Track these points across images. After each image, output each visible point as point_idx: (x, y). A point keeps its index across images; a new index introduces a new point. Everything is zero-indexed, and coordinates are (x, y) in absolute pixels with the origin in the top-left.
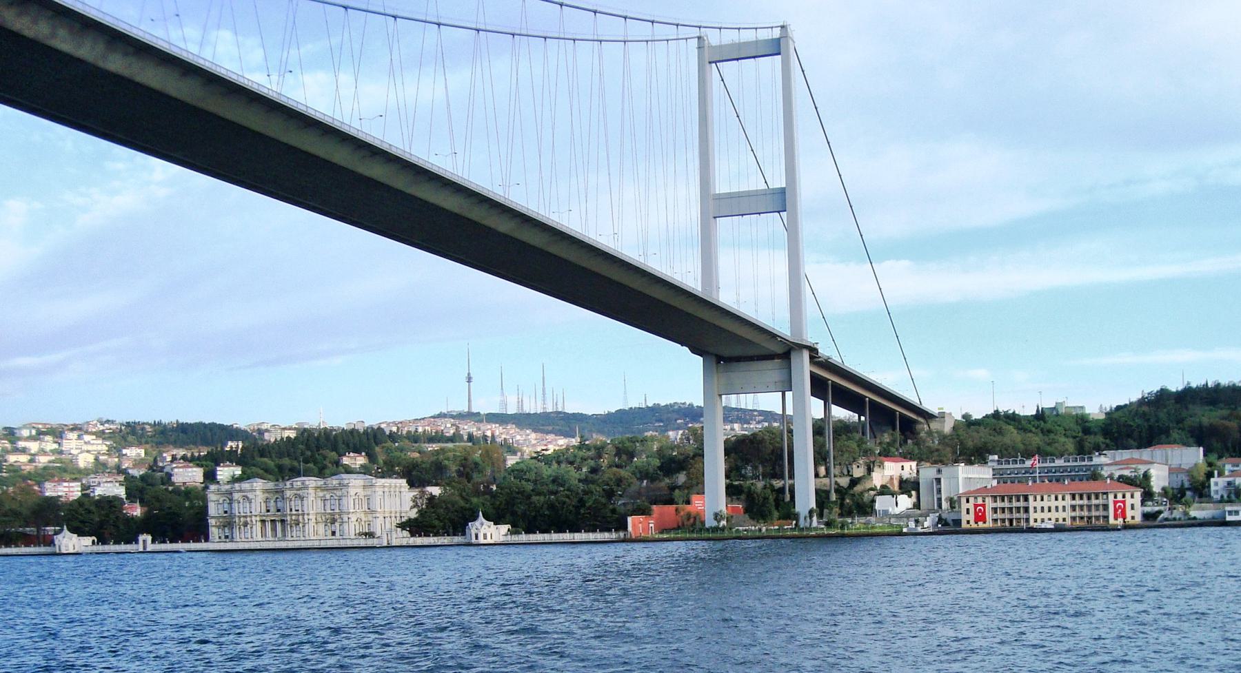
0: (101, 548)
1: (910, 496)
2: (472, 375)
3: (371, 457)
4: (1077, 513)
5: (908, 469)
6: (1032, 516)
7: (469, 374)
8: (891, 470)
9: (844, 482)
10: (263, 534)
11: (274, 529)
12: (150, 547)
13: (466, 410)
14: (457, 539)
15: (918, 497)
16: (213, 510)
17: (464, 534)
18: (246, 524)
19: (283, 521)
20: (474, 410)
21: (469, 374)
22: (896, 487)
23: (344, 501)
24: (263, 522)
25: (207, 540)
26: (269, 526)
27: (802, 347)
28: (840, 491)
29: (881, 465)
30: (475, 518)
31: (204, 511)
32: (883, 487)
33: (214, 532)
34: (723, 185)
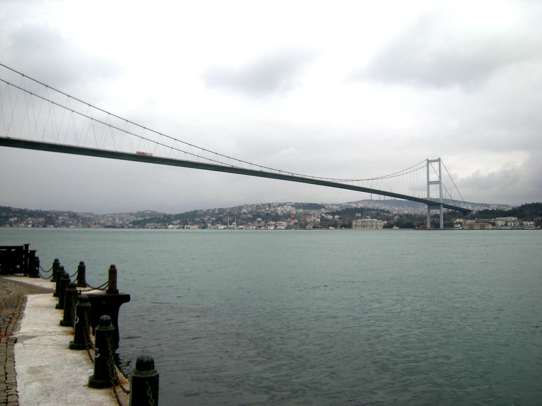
0: (335, 229)
1: (460, 225)
3: (362, 214)
4: (481, 228)
5: (461, 220)
6: (474, 228)
8: (458, 220)
9: (450, 222)
10: (362, 228)
11: (363, 227)
12: (344, 229)
13: (370, 199)
14: (391, 229)
15: (462, 225)
16: (353, 224)
17: (392, 228)
18: (359, 226)
19: (365, 226)
20: (372, 199)
22: (458, 223)
23: (374, 223)
24: (361, 226)
25: (352, 228)
26: (362, 226)
27: (441, 204)
28: (449, 223)
29: (456, 220)
30: (394, 226)
31: (352, 223)
32: (456, 223)
33: (353, 227)
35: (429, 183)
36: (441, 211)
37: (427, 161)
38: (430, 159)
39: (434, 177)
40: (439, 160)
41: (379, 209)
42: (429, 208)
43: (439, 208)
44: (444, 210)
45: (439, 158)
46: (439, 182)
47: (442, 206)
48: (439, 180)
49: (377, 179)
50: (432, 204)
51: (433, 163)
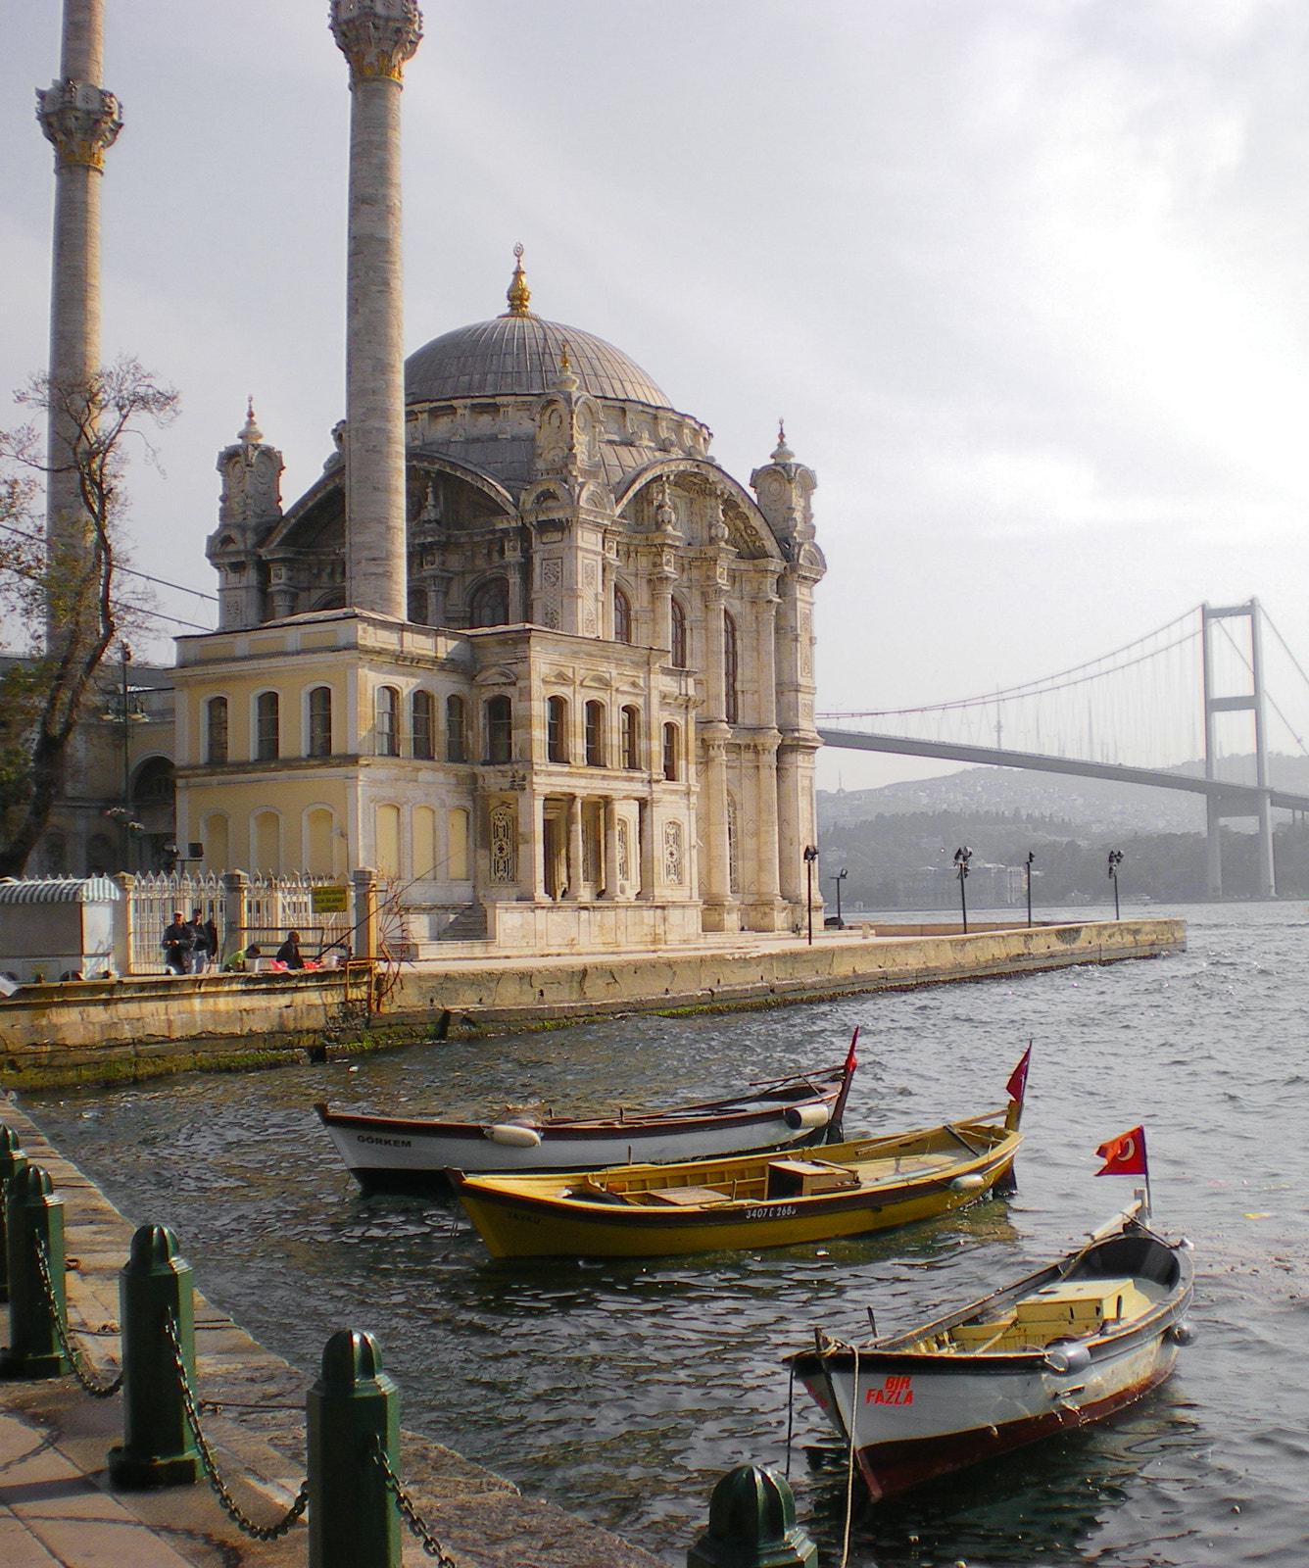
2: (1003, 722)
7: (999, 722)
21: (999, 722)
34: (1220, 691)
35: (1212, 705)
36: (1262, 822)
37: (1203, 610)
38: (1216, 603)
39: (1232, 681)
40: (1249, 609)
41: (1024, 817)
42: (1213, 812)
43: (1256, 810)
44: (1275, 815)
45: (1252, 601)
46: (1251, 703)
47: (1268, 801)
48: (1252, 694)
49: (964, 704)
50: (1222, 797)
51: (1226, 622)
